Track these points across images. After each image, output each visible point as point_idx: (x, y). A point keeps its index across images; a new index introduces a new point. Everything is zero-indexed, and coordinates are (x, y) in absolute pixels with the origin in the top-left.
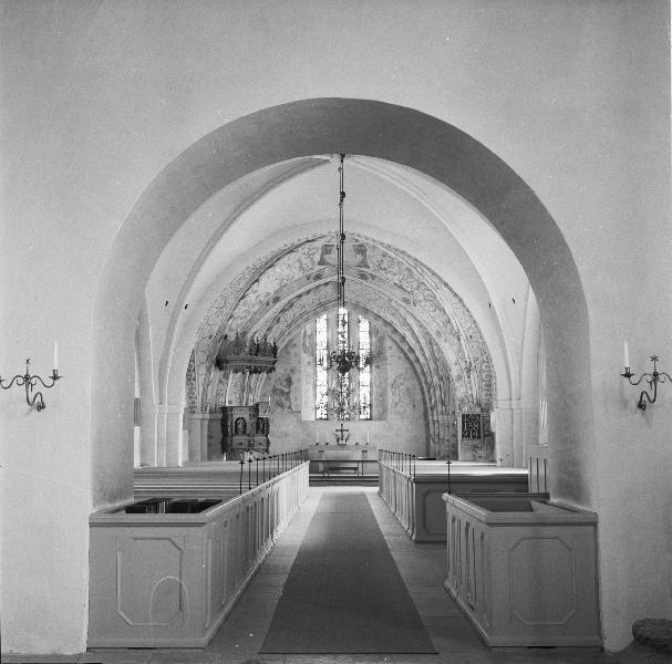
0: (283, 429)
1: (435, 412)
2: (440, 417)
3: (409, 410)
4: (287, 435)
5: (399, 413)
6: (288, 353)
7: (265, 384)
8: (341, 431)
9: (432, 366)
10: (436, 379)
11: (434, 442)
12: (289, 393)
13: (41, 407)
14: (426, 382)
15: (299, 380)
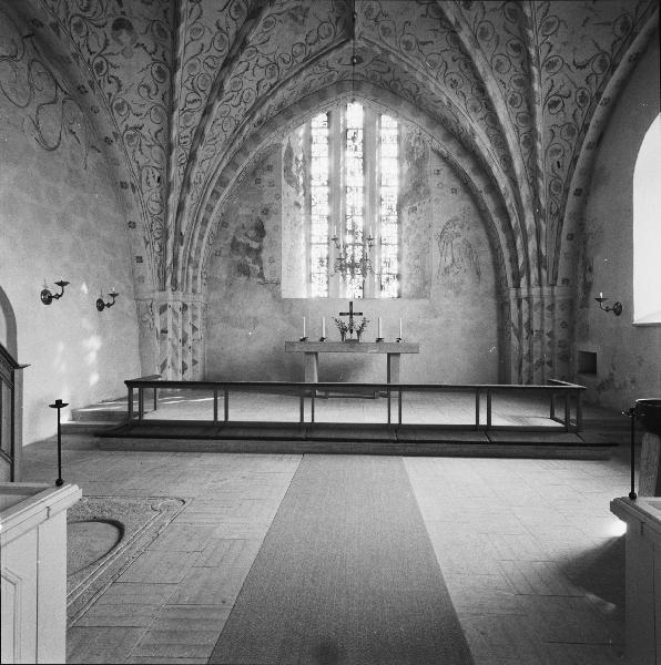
0: (250, 311)
1: (523, 281)
2: (535, 291)
3: (468, 280)
4: (256, 322)
5: (451, 285)
6: (258, 181)
7: (215, 237)
8: (351, 314)
9: (525, 191)
10: (529, 220)
11: (519, 336)
12: (259, 250)
13: (101, 306)
14: (508, 227)
15: (277, 228)
